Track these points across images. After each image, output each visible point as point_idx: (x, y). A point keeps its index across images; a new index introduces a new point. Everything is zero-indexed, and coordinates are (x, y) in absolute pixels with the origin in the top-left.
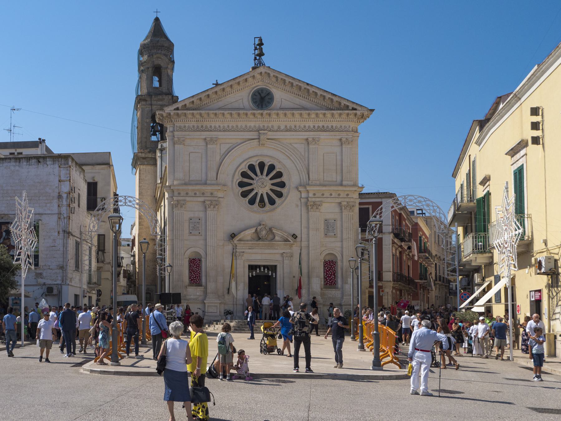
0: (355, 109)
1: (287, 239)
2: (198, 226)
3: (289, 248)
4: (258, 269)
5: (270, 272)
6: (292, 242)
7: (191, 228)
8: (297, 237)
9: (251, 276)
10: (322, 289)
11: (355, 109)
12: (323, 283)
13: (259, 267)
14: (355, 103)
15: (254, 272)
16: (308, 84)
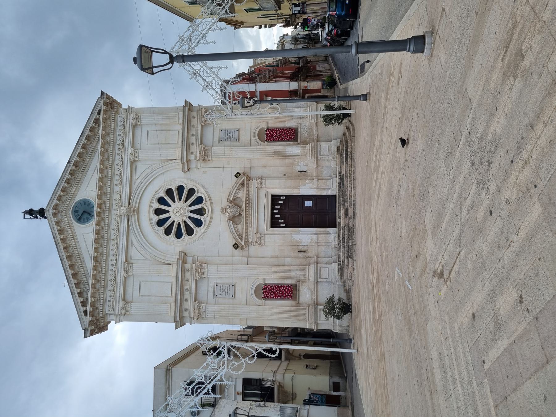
0: (100, 111)
2: (224, 288)
3: (251, 181)
4: (276, 216)
5: (280, 202)
6: (244, 178)
7: (227, 296)
8: (238, 173)
9: (284, 225)
10: (298, 144)
11: (100, 111)
12: (292, 143)
13: (273, 214)
14: (92, 112)
15: (280, 221)
16: (69, 162)
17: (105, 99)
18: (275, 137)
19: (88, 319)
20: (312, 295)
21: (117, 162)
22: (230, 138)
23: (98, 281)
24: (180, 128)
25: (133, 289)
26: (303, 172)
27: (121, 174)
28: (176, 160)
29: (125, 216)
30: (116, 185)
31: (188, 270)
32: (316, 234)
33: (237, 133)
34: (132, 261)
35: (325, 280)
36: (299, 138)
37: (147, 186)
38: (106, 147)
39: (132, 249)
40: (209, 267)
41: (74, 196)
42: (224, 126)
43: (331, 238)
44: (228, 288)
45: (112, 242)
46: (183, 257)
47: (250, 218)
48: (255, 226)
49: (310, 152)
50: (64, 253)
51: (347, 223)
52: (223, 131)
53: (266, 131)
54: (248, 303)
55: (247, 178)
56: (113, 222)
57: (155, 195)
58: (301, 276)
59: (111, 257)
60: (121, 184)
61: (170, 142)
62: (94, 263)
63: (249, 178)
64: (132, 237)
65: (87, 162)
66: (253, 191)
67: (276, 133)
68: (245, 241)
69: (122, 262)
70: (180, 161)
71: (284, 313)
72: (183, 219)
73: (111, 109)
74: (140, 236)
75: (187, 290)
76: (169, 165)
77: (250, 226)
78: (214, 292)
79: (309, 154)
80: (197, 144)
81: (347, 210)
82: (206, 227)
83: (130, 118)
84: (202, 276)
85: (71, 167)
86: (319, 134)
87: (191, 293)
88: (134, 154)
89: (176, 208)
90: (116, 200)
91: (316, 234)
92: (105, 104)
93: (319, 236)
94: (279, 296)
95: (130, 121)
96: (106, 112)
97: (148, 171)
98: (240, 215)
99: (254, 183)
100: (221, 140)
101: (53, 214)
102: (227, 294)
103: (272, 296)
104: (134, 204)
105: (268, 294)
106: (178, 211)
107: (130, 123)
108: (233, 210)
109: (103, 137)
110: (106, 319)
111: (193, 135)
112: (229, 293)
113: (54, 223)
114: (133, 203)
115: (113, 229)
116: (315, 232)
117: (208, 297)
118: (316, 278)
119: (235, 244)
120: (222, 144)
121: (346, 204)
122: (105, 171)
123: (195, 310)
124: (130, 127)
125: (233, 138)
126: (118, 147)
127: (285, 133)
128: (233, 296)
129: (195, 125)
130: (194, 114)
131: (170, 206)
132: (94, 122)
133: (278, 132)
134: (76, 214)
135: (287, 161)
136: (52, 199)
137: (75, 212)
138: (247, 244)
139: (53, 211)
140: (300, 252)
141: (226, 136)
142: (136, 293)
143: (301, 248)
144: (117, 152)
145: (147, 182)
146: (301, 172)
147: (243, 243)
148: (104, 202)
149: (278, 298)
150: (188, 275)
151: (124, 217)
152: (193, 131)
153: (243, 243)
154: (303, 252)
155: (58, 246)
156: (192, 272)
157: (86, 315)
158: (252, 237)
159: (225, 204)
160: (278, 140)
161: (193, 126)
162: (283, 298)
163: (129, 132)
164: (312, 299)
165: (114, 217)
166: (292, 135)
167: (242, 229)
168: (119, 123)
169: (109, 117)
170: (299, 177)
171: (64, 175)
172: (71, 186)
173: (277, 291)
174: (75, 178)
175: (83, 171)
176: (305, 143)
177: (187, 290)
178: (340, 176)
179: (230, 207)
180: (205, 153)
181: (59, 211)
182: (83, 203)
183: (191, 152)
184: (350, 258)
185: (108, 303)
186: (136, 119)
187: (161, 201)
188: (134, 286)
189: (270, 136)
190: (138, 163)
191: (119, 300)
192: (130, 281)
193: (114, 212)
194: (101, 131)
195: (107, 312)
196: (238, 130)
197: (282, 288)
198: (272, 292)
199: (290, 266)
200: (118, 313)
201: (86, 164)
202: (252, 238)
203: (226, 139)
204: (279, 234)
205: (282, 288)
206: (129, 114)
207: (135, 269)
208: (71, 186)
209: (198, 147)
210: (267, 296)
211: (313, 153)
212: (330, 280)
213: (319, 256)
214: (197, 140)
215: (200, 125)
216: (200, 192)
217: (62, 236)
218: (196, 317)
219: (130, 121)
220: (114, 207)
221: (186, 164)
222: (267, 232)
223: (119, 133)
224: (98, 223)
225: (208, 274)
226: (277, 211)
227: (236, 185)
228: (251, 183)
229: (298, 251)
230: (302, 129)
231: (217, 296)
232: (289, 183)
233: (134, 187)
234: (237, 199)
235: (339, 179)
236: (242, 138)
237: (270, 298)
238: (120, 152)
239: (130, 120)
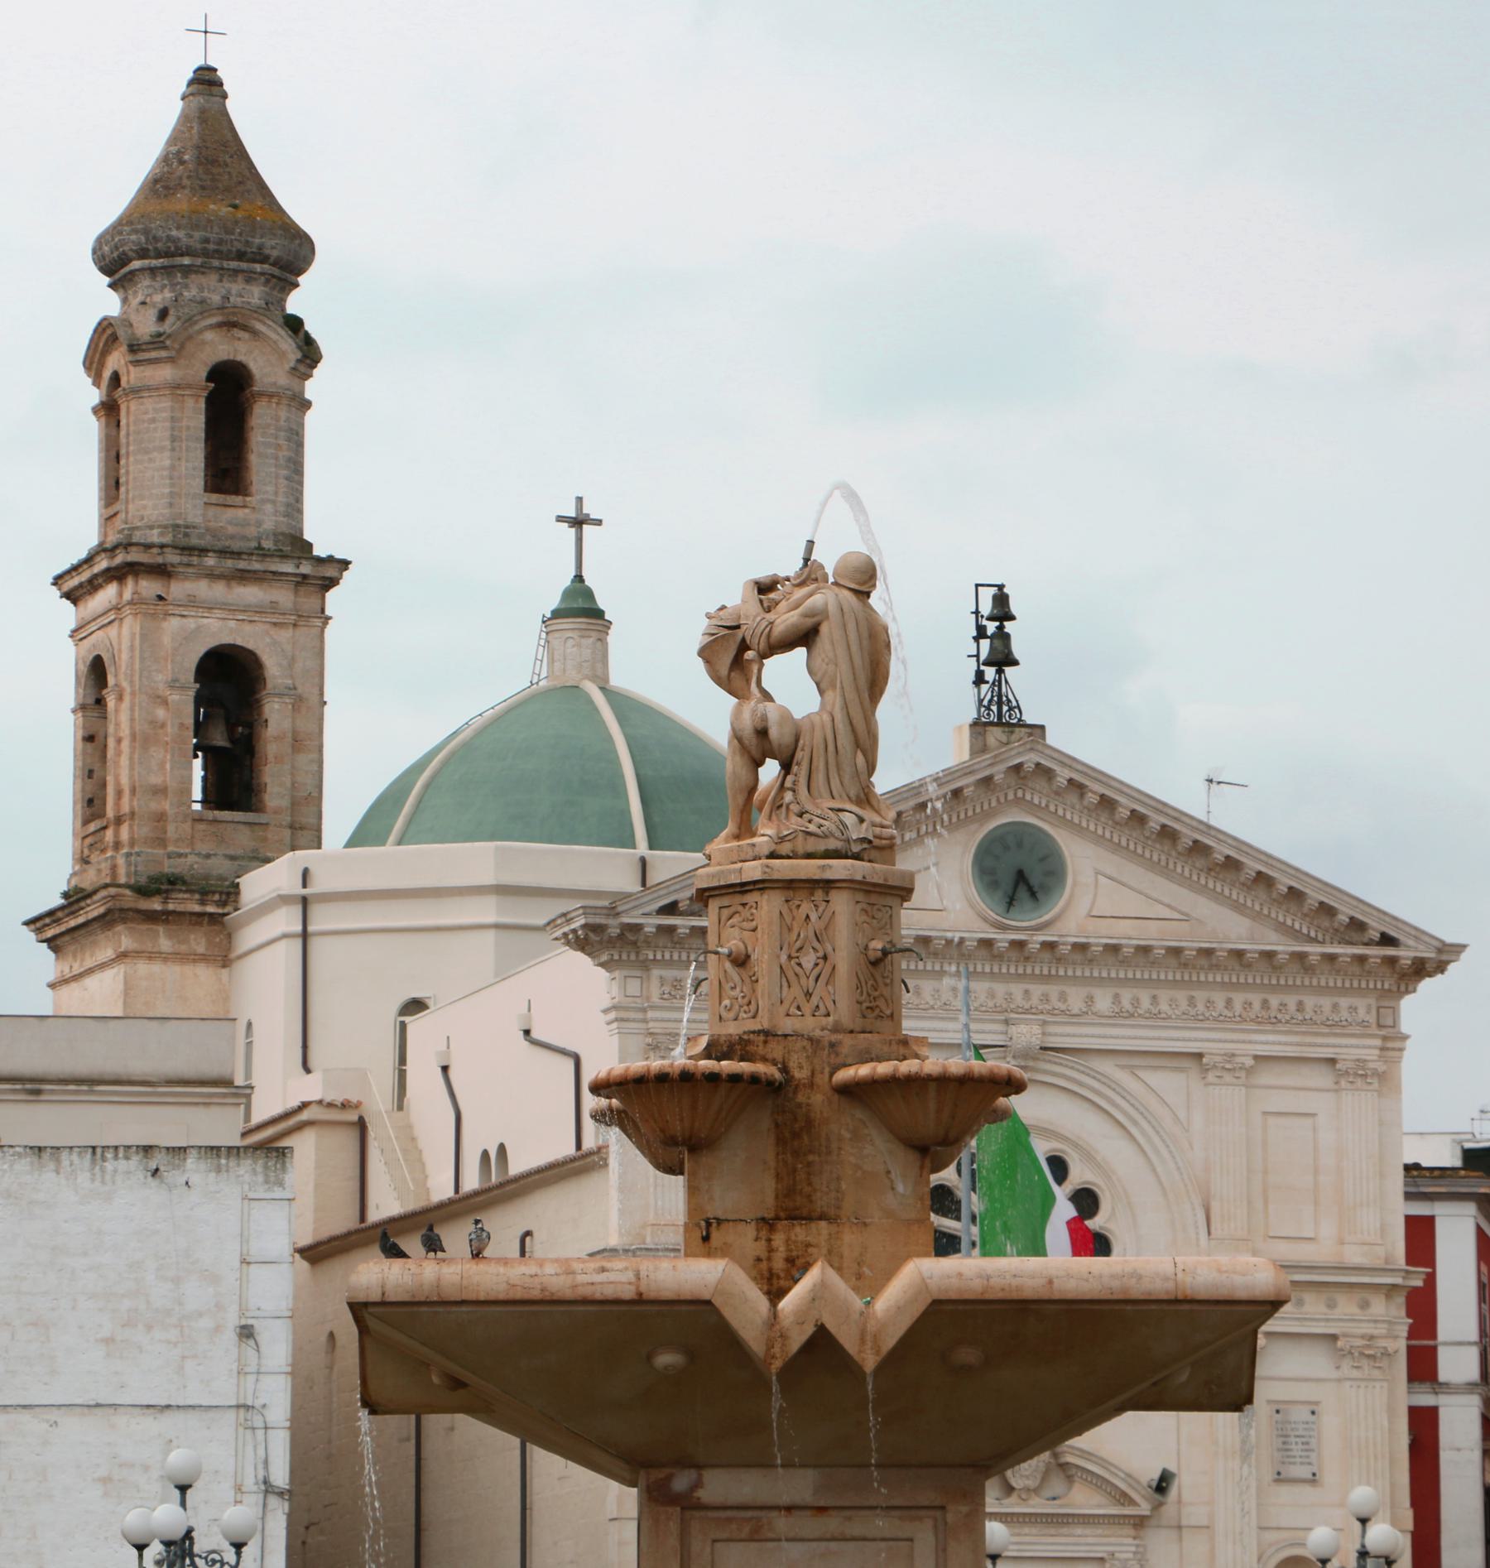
3: (1132, 1532)
6: (1144, 1508)
22: (1285, 1448)
27: (1156, 1016)
28: (1209, 1233)
30: (1117, 996)
33: (1304, 1472)
41: (1077, 829)
42: (1330, 1425)
52: (1313, 1418)
60: (1118, 1015)
88: (1230, 1066)
90: (1063, 997)
96: (1392, 961)
100: (1278, 1412)
129: (1337, 1313)
141: (1292, 1430)
145: (1125, 1113)
168: (1344, 1002)
186: (1361, 1074)
196: (1313, 1480)
203: (1284, 1433)
227: (1122, 1475)
233: (1106, 1066)
236: (1285, 1492)
238: (1238, 1007)
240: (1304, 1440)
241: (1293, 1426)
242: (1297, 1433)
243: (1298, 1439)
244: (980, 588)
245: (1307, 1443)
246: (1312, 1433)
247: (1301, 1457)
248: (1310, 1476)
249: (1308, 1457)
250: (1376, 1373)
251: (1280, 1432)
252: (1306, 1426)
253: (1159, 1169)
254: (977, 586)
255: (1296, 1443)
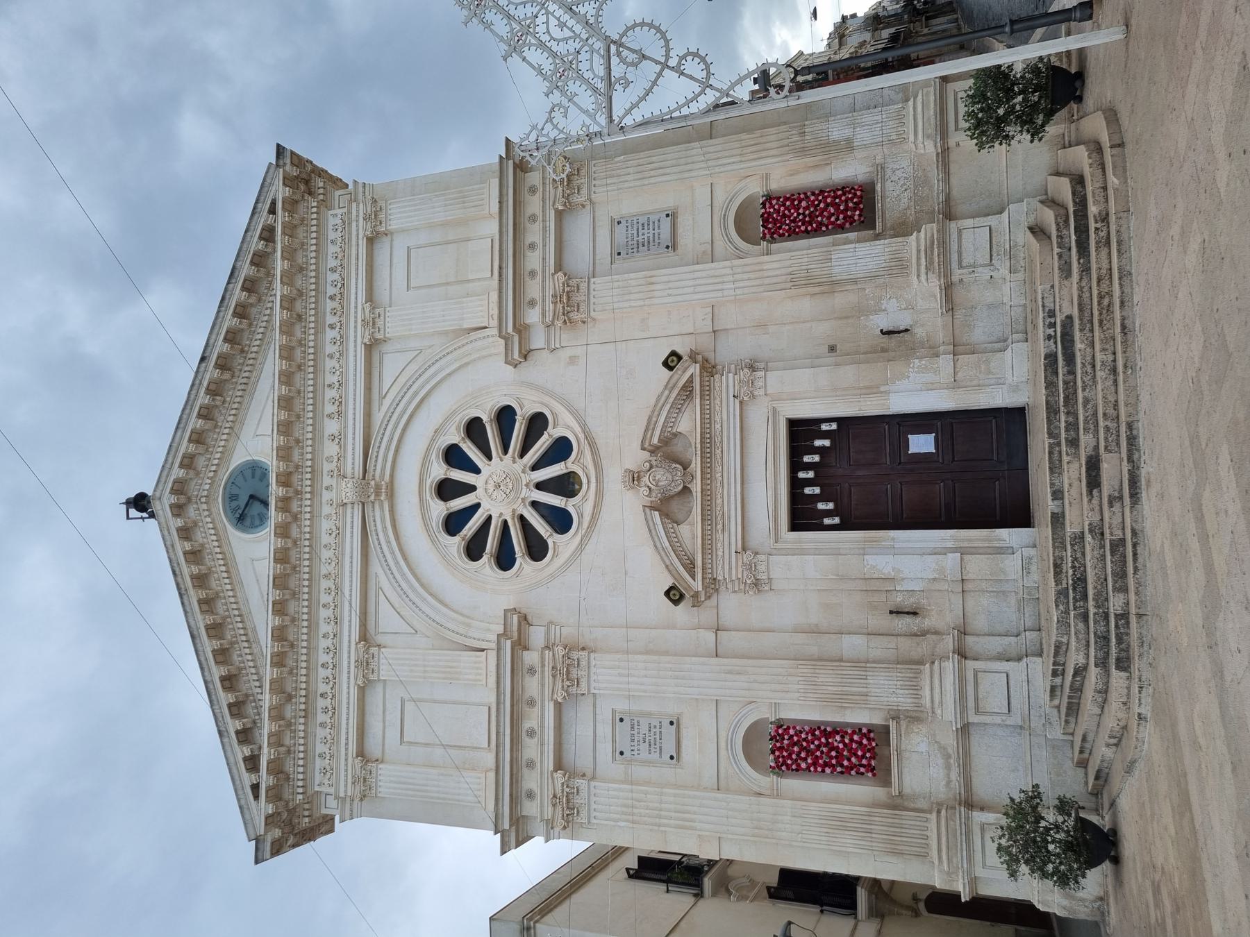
0: (274, 203)
1: (684, 387)
2: (644, 729)
3: (717, 377)
4: (808, 491)
5: (818, 443)
6: (695, 369)
7: (656, 756)
8: (673, 353)
9: (837, 520)
10: (877, 237)
11: (274, 203)
13: (796, 485)
14: (255, 208)
15: (821, 506)
16: (203, 359)
17: (288, 168)
18: (794, 221)
19: (263, 811)
20: (948, 767)
21: (330, 349)
22: (647, 244)
23: (290, 698)
24: (492, 228)
25: (384, 722)
26: (899, 332)
28: (486, 328)
29: (356, 506)
30: (329, 416)
31: (532, 671)
32: (954, 550)
33: (666, 224)
34: (380, 639)
35: (998, 720)
36: (878, 214)
37: (411, 416)
38: (298, 306)
39: (377, 604)
40: (593, 663)
41: (226, 454)
43: (1012, 565)
44: (658, 730)
45: (325, 584)
46: (515, 628)
47: (719, 501)
48: (735, 528)
49: (923, 260)
50: (199, 616)
51: (1091, 517)
52: (623, 222)
53: (764, 207)
54: (722, 783)
55: (703, 368)
56: (326, 525)
57: (433, 440)
58: (903, 700)
59: (324, 628)
60: (339, 413)
61: (470, 277)
62: (273, 647)
63: (709, 368)
64: (376, 567)
65: (253, 355)
66: (726, 412)
67: (797, 209)
68: (703, 578)
69: (350, 641)
70: (495, 331)
71: (845, 829)
72: (514, 511)
73: (306, 196)
74: (397, 563)
75: (531, 733)
76: (470, 346)
77: (720, 527)
78: (614, 741)
79: (919, 265)
80: (544, 271)
81: (1093, 465)
82: (582, 532)
83: (358, 216)
84: (574, 690)
85: (209, 373)
86: (955, 193)
87: (542, 744)
88: (371, 323)
89: (494, 477)
90: (329, 460)
91: (954, 550)
92: (287, 181)
93: (967, 557)
94: (826, 765)
95: (357, 226)
96: (291, 205)
97: (413, 367)
98: (686, 490)
99: (727, 384)
100: (619, 254)
101: (171, 506)
102: (653, 750)
103: (803, 765)
104: (379, 469)
105: (790, 756)
106: (498, 486)
107: (360, 229)
108: (663, 477)
109: (288, 278)
110: (318, 808)
111: (532, 246)
112: (661, 749)
113: (175, 533)
114: (375, 466)
115: (325, 546)
116: (950, 545)
117: (595, 758)
118: (963, 709)
119: (671, 588)
120: (620, 264)
121: (1086, 440)
122: (298, 378)
123: (555, 796)
124: (360, 242)
125: (657, 241)
126: (330, 305)
127: (827, 205)
128: (672, 758)
129: (538, 212)
130: (534, 178)
131: (477, 471)
132: (261, 238)
133: (804, 204)
134: (234, 504)
135: (841, 300)
136: (168, 466)
137: (231, 498)
138: (713, 585)
139: (173, 499)
140: (898, 613)
141: (633, 240)
142: (393, 735)
143: (899, 600)
144: (330, 319)
145: (409, 403)
146: (889, 333)
147: (697, 585)
148: (297, 467)
149: (823, 771)
150: (532, 686)
151: (353, 508)
152: (533, 234)
153: (697, 585)
154: (908, 613)
155: (185, 597)
156: (543, 678)
157: (256, 797)
158: (728, 566)
159: (635, 458)
160: (806, 231)
161: (533, 218)
162: (842, 773)
163: (357, 259)
164: (949, 782)
165: (326, 510)
166: (854, 209)
167: (694, 537)
168: (332, 235)
169: (303, 220)
170: (884, 350)
171: (192, 397)
172: (216, 426)
173: (818, 747)
174: (224, 402)
175: (245, 381)
176: (902, 229)
177: (531, 733)
178: (1053, 325)
179: (651, 467)
180: (569, 298)
181: (189, 499)
182: (248, 473)
183: (527, 299)
184: (1119, 668)
185: (319, 763)
186: (375, 215)
187: (453, 456)
188: (387, 713)
189: (775, 221)
190: (386, 348)
191: (347, 754)
192: (375, 699)
193: (326, 496)
194: (279, 261)
195: (317, 789)
196: (672, 215)
197: (838, 738)
198: (802, 749)
199: (862, 664)
200: (346, 791)
201: (251, 362)
202: (726, 567)
203: (635, 246)
204: (818, 552)
205: (838, 738)
206: (354, 205)
207: (388, 664)
208: (216, 426)
209: (549, 284)
210: (784, 763)
211: (932, 263)
212: (1015, 719)
213: (968, 629)
214: (544, 259)
215: (553, 212)
216: (561, 422)
217: (195, 570)
218: (559, 822)
219: (357, 226)
220: (327, 481)
221: (516, 338)
222: (778, 546)
223: (332, 263)
224: (283, 531)
225: (593, 684)
226: (811, 474)
227: (667, 392)
228: (717, 385)
229: (891, 612)
230: (888, 184)
231: (622, 753)
232: (849, 374)
233: (378, 417)
234: (675, 441)
235: (1049, 337)
236: (684, 240)
237: (797, 770)
238: (334, 320)
239: (357, 221)
240: (640, 228)
241: (629, 239)
242: (635, 235)
243: (640, 234)
244: (130, 516)
245: (643, 224)
246: (635, 222)
247: (654, 230)
248: (669, 218)
249: (654, 223)
250: (583, 172)
251: (635, 250)
252: (630, 227)
253: (448, 371)
254: (128, 518)
255: (643, 234)
